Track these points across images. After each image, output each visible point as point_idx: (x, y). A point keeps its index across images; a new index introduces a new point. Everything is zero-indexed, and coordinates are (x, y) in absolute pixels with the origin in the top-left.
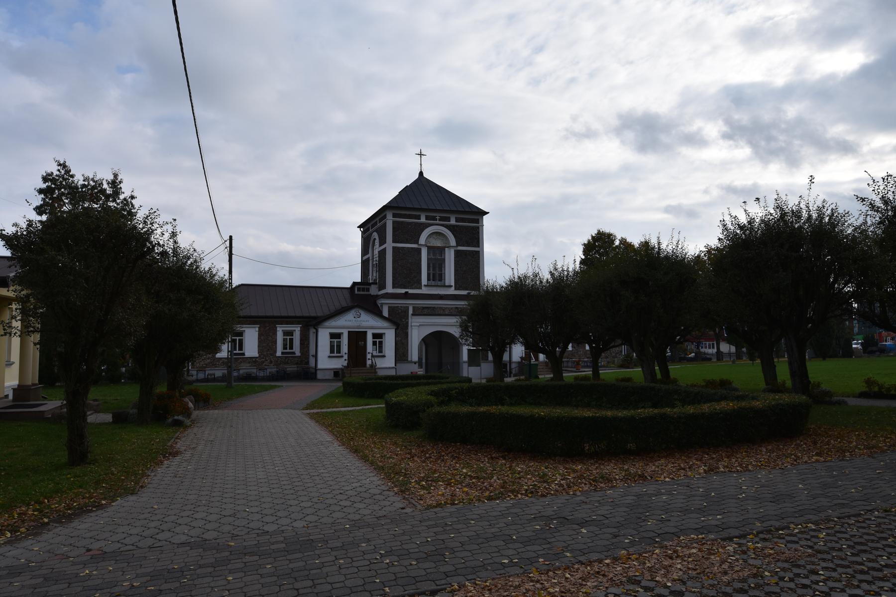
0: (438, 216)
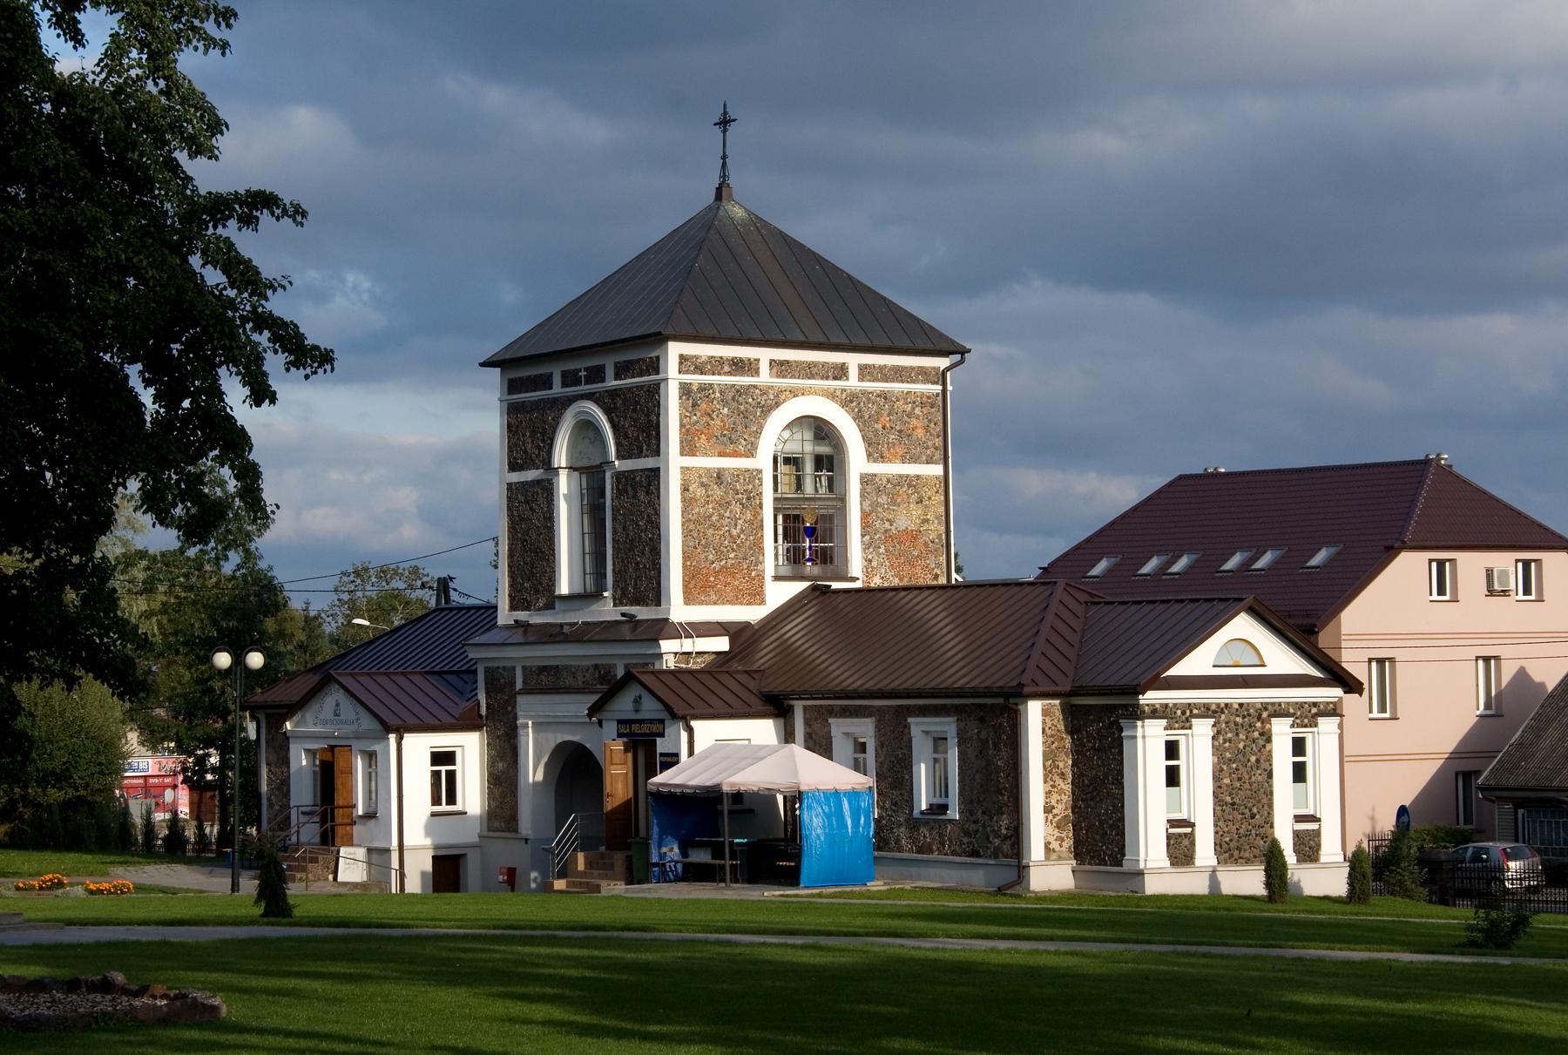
0: (581, 365)
